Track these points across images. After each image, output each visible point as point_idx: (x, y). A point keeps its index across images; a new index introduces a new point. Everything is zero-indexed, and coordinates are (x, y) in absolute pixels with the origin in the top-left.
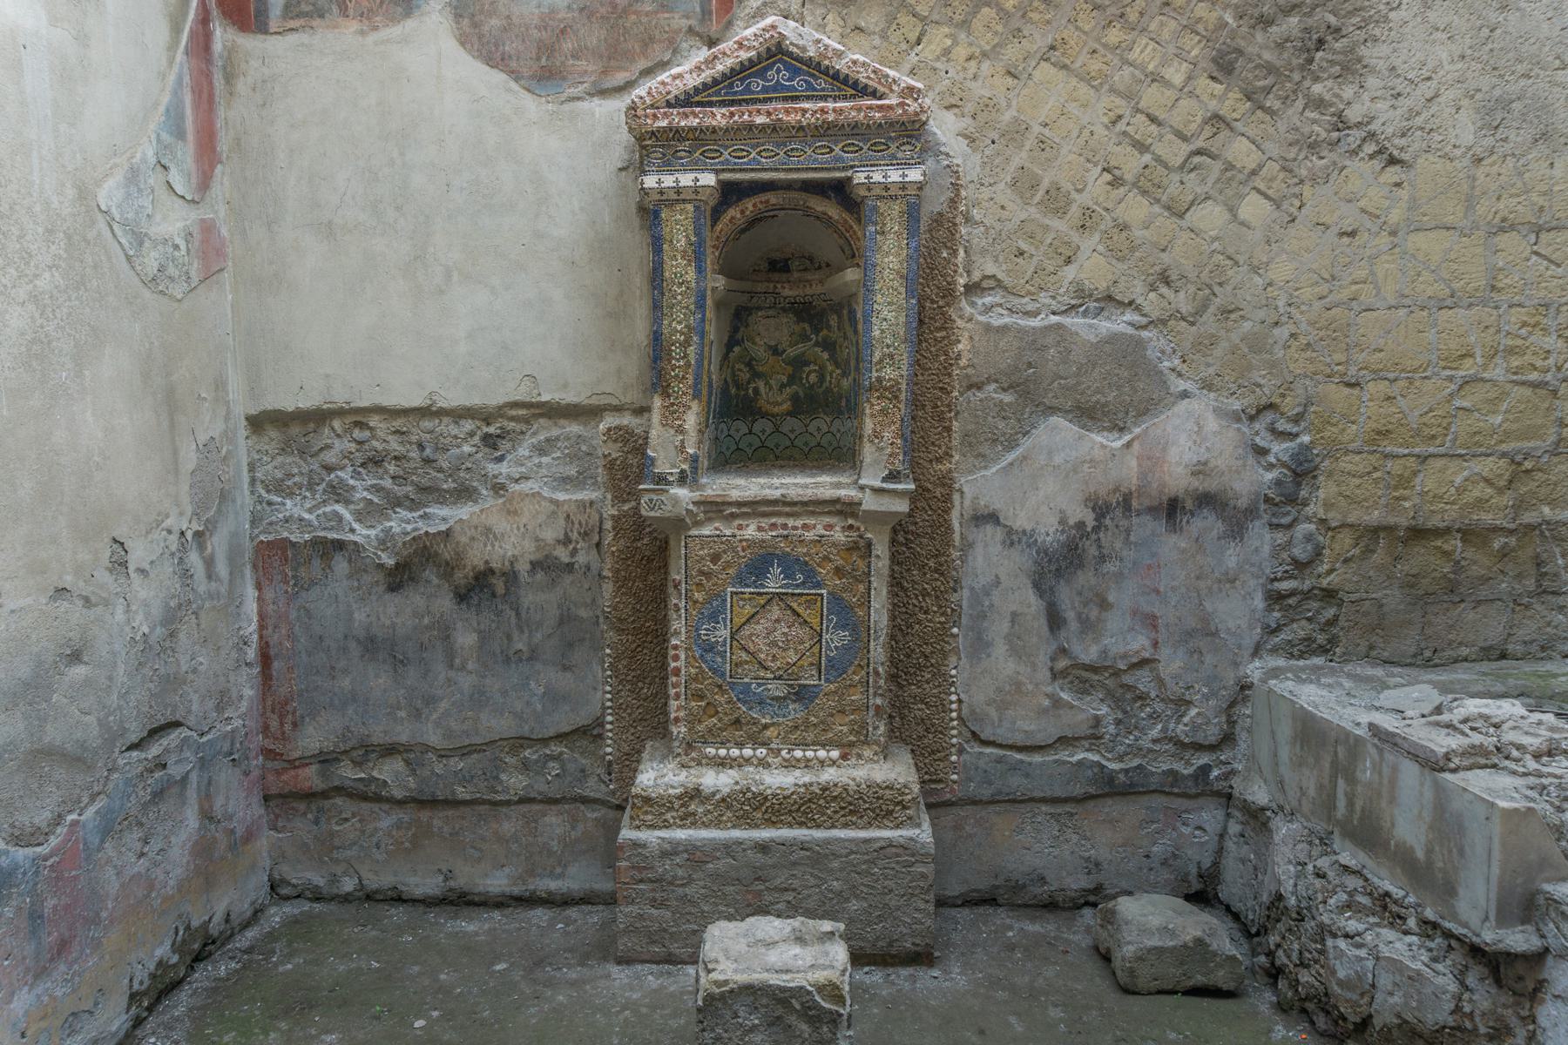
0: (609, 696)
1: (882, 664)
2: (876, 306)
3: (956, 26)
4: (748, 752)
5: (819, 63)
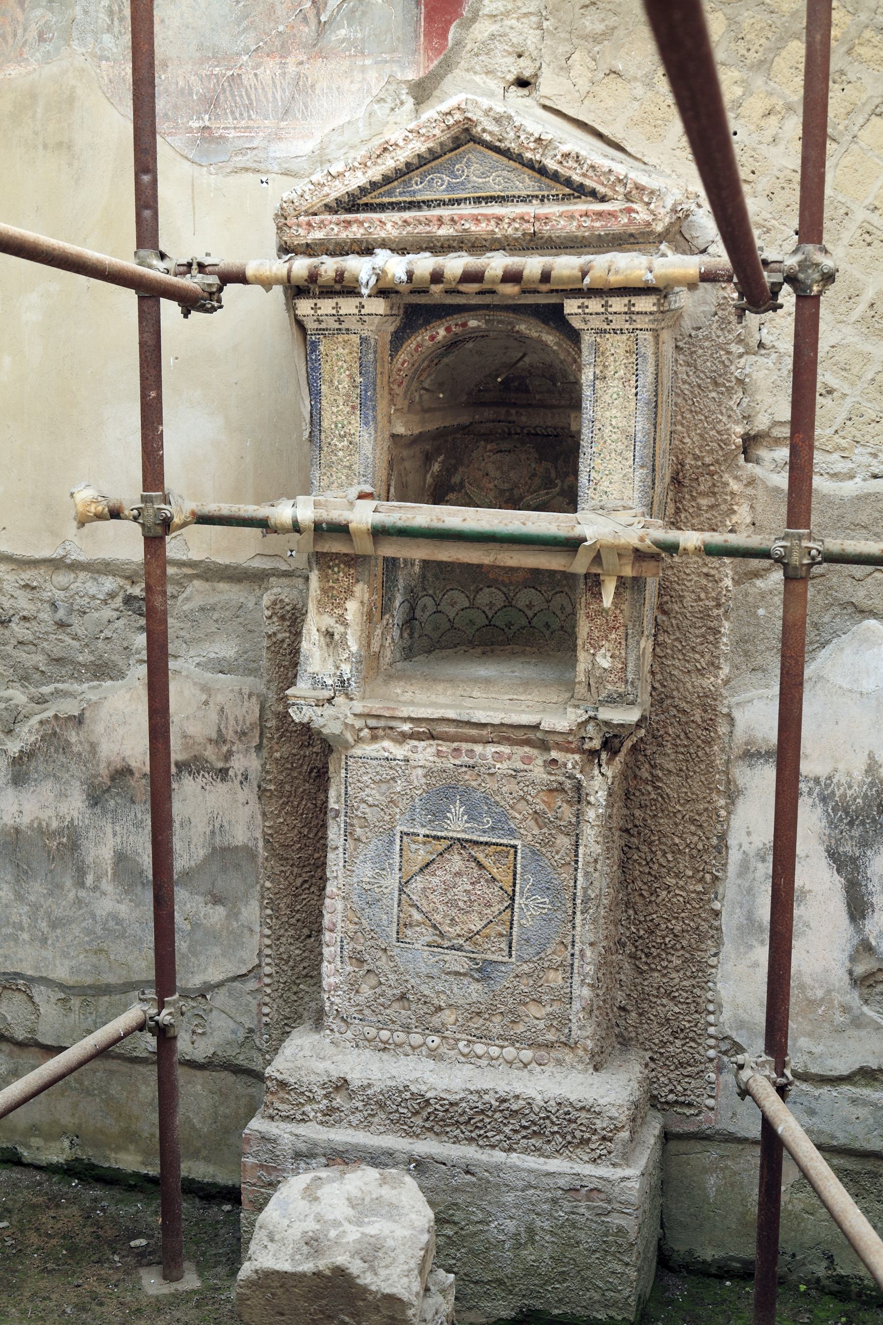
0: (268, 942)
1: (591, 944)
2: (593, 474)
3: (751, 68)
4: (416, 1039)
5: (520, 155)
